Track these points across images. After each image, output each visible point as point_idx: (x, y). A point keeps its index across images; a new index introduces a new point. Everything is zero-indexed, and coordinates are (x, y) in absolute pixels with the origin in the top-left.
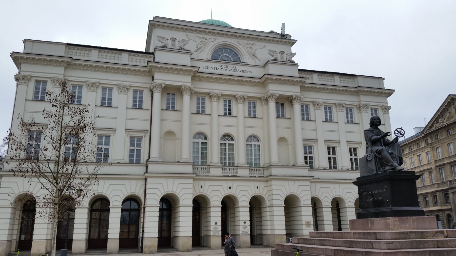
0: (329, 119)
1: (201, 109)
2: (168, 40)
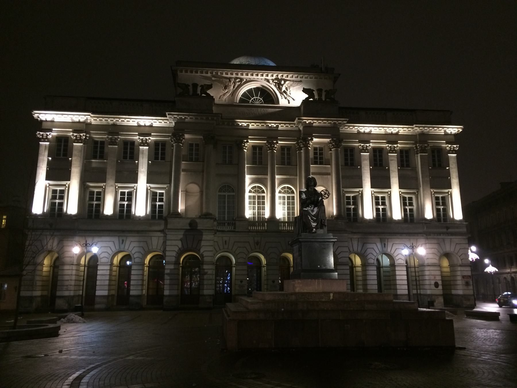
2: (189, 86)
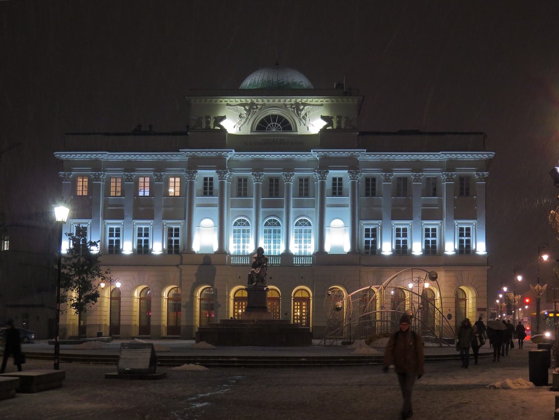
2: (202, 118)
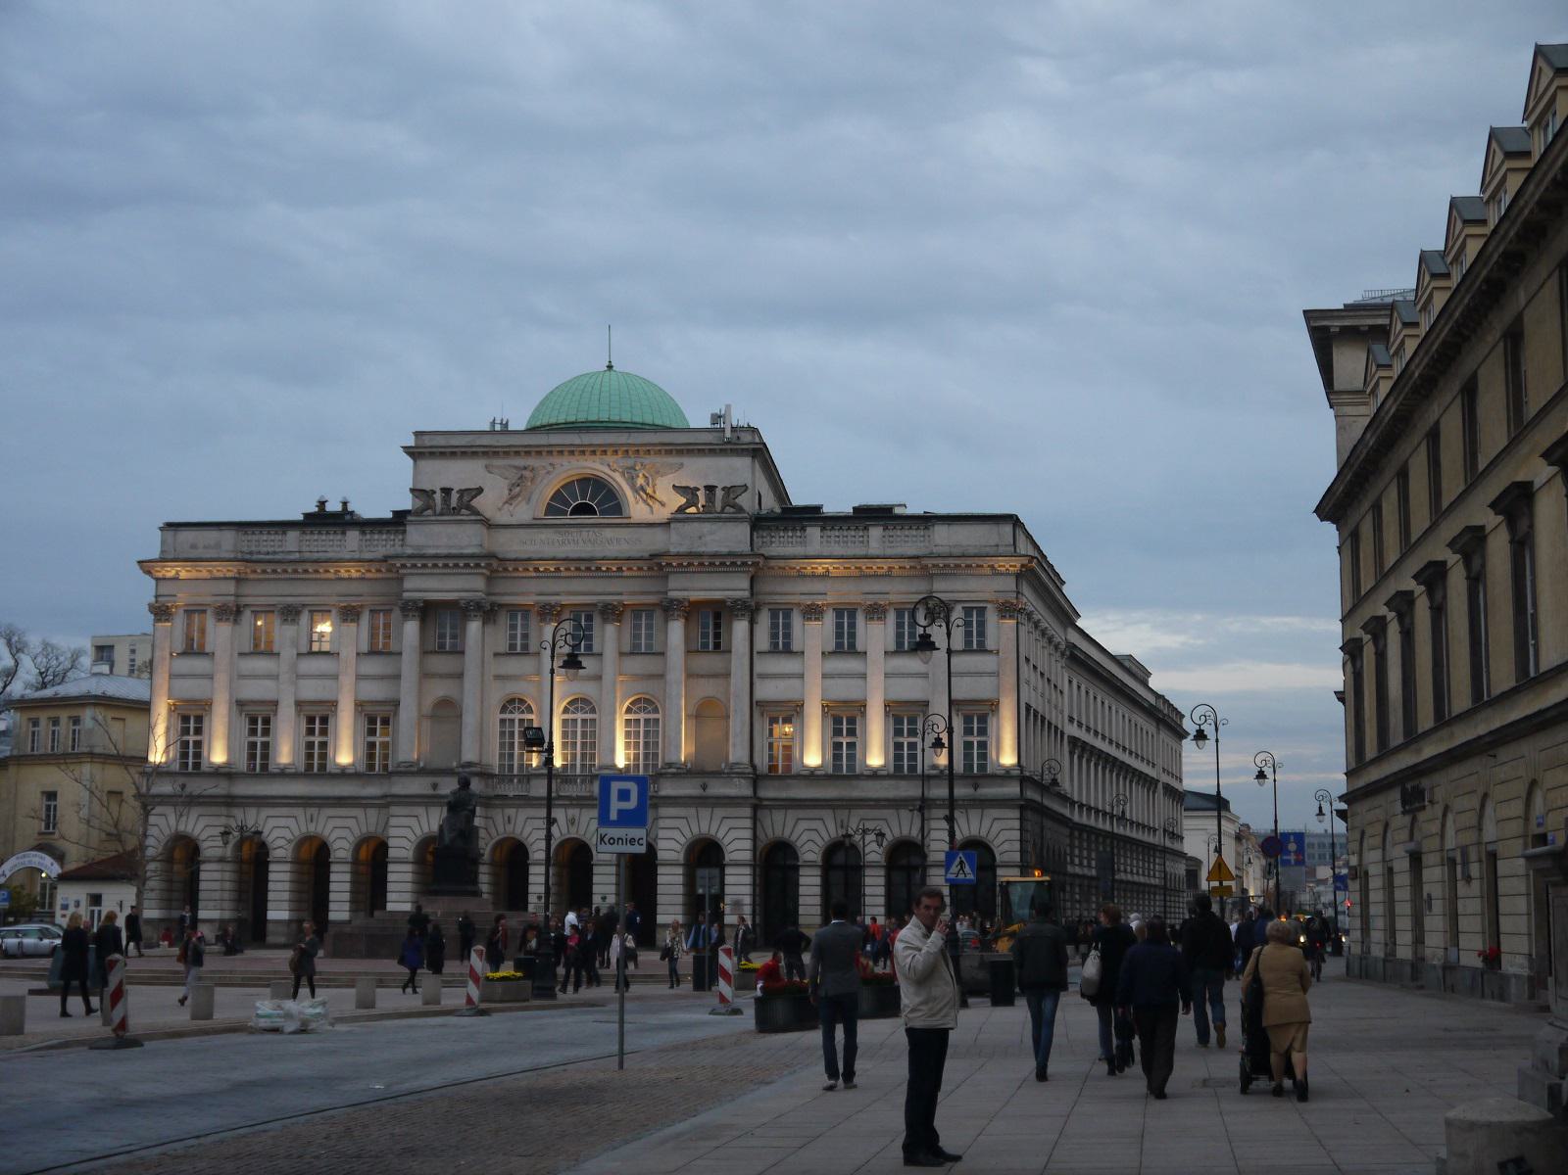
0: (845, 646)
1: (519, 642)
2: (434, 492)
